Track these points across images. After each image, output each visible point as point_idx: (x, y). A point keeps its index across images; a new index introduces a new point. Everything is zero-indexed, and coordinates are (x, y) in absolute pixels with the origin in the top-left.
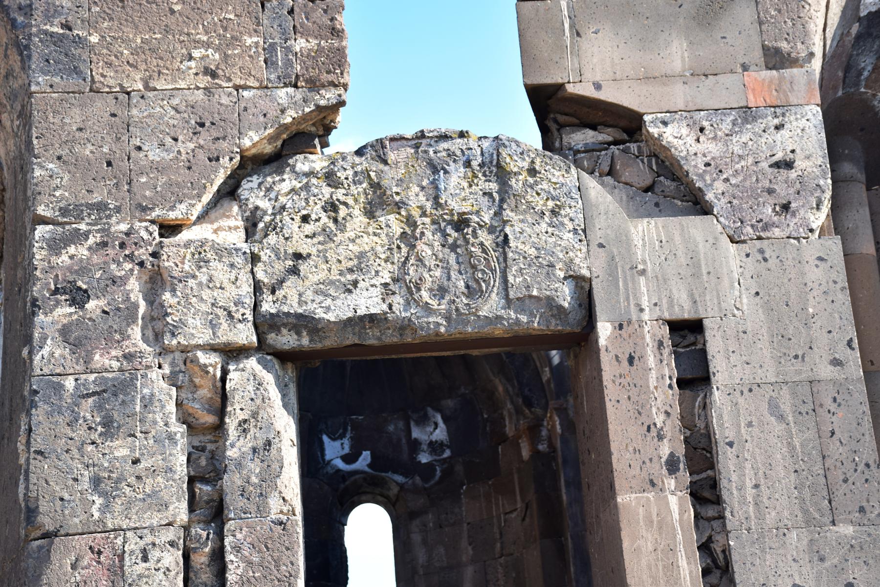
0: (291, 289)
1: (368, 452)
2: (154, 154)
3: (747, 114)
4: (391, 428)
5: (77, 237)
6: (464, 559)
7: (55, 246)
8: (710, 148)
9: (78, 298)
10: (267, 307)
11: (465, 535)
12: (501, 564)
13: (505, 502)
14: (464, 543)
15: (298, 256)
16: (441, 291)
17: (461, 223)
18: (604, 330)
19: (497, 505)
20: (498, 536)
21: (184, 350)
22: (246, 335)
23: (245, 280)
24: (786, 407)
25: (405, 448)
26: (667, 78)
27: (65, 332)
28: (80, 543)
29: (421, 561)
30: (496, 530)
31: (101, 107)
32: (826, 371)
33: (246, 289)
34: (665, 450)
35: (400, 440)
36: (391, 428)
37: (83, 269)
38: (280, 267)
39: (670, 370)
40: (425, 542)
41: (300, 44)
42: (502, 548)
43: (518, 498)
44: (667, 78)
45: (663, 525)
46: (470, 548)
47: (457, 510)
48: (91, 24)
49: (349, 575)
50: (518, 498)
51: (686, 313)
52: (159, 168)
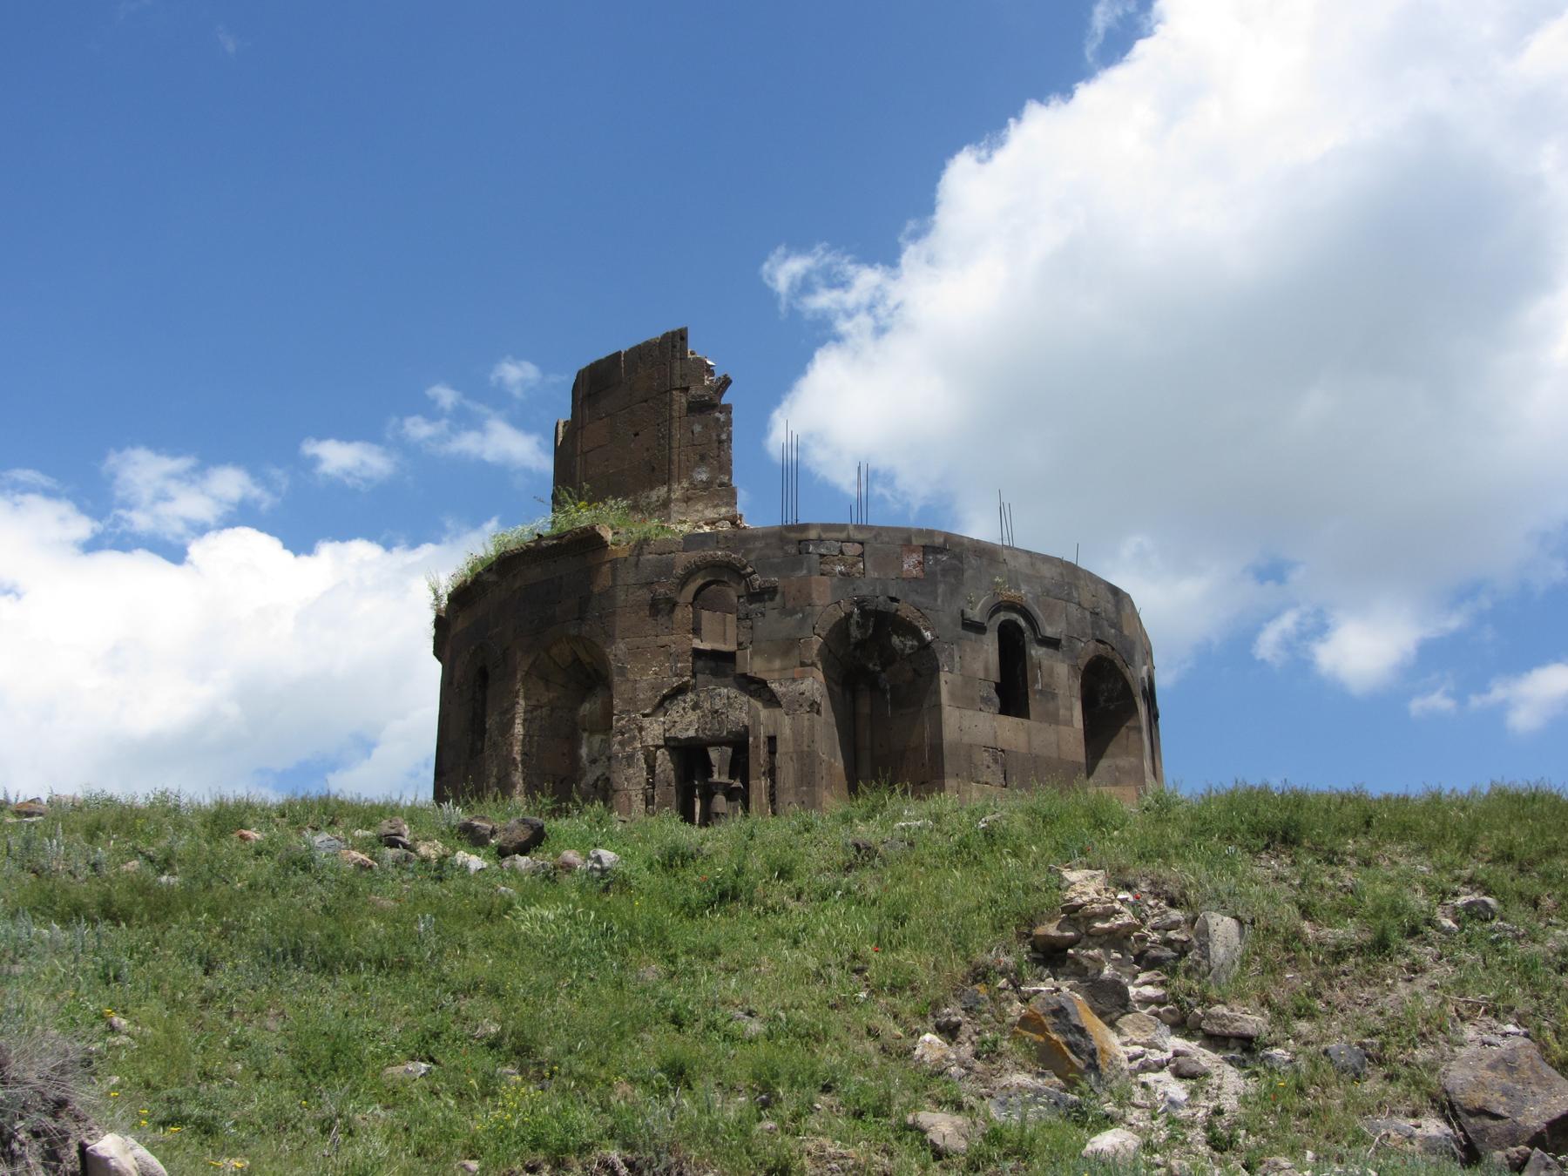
0: (672, 731)
2: (642, 696)
3: (794, 680)
5: (623, 719)
7: (618, 721)
8: (783, 689)
9: (623, 734)
10: (667, 735)
15: (675, 722)
16: (710, 730)
17: (716, 712)
18: (751, 739)
21: (647, 746)
22: (661, 742)
23: (662, 728)
24: (795, 757)
26: (773, 671)
27: (619, 743)
28: (622, 793)
31: (630, 684)
32: (806, 749)
33: (662, 731)
34: (763, 770)
37: (624, 726)
38: (671, 724)
39: (766, 749)
41: (679, 665)
44: (773, 671)
45: (760, 789)
48: (629, 663)
51: (772, 734)
52: (643, 700)
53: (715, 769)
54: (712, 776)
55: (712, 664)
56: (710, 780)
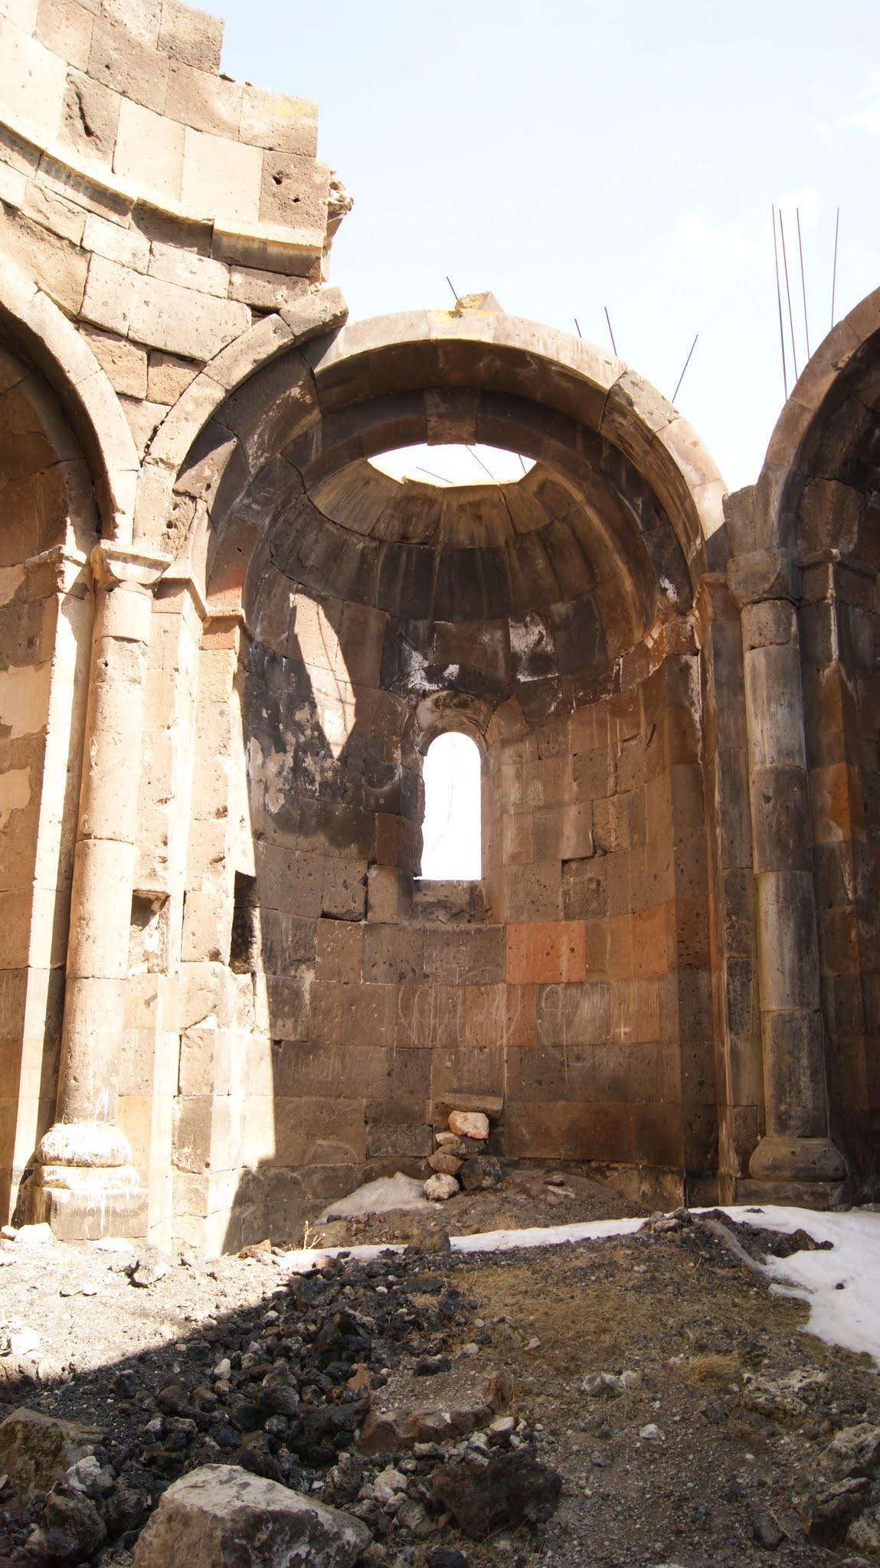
1: (457, 666)
4: (486, 638)
6: (566, 798)
11: (570, 769)
12: (613, 803)
13: (624, 727)
14: (568, 778)
19: (613, 730)
20: (612, 770)
25: (502, 663)
29: (512, 798)
30: (610, 762)
35: (496, 653)
36: (486, 638)
40: (518, 775)
42: (616, 785)
43: (643, 719)
46: (575, 784)
47: (561, 738)
49: (426, 812)
50: (643, 719)
53: (123, 522)
54: (112, 537)
55: (137, 239)
56: (105, 544)
